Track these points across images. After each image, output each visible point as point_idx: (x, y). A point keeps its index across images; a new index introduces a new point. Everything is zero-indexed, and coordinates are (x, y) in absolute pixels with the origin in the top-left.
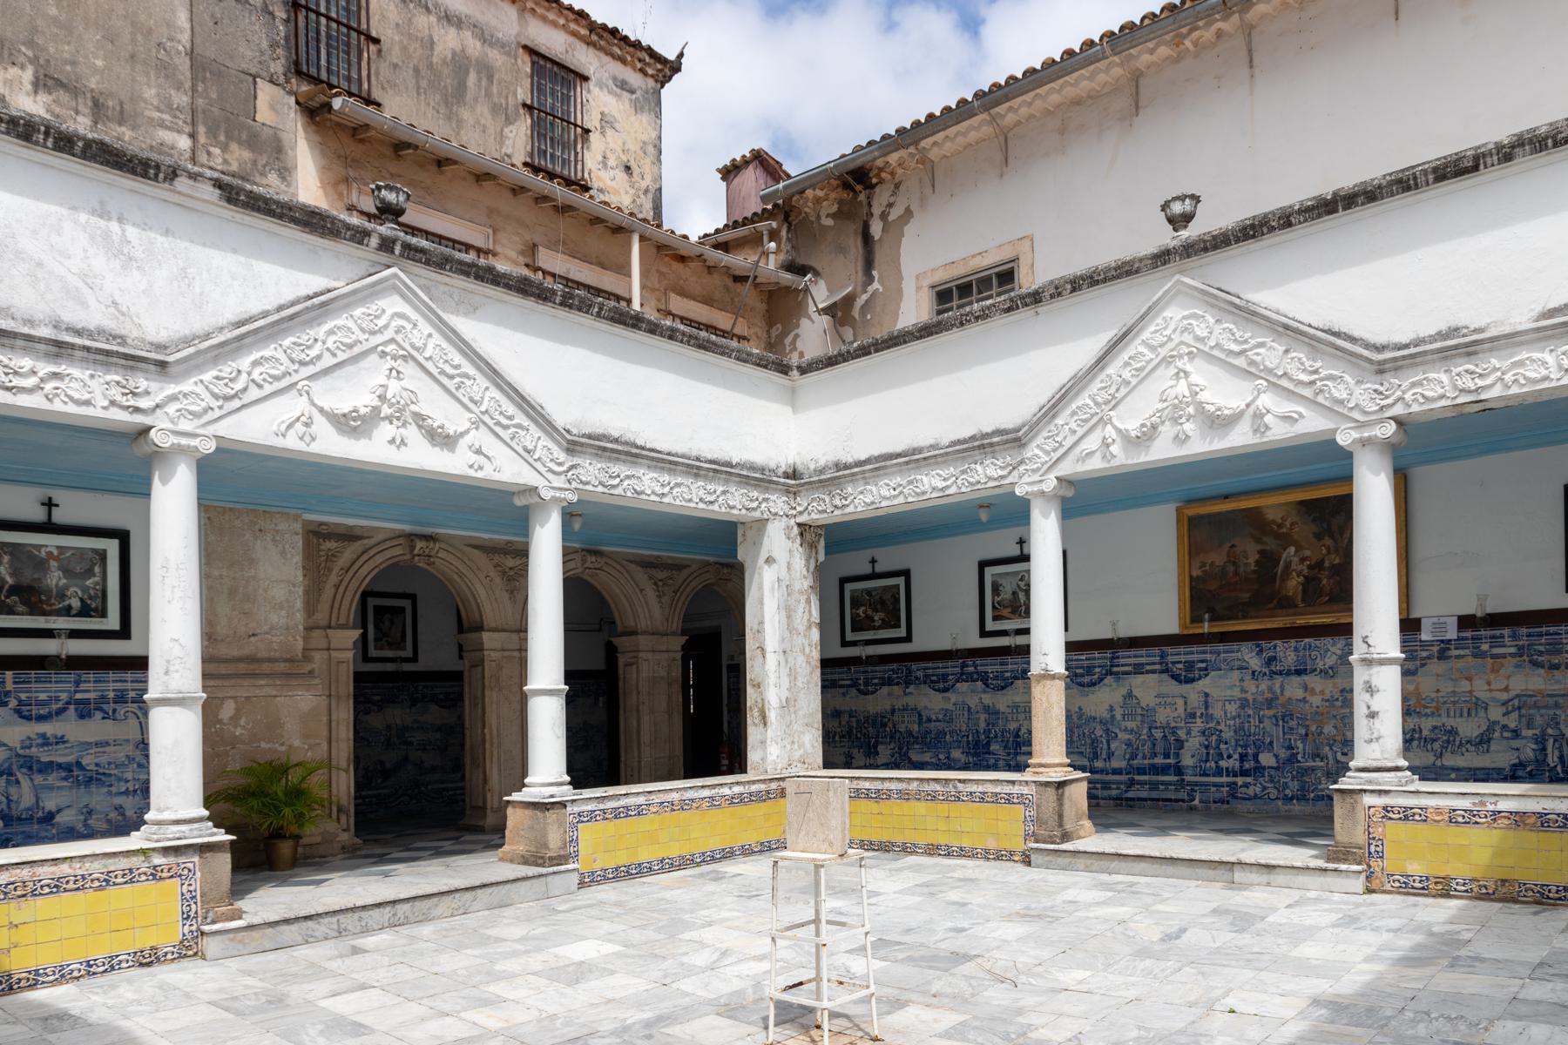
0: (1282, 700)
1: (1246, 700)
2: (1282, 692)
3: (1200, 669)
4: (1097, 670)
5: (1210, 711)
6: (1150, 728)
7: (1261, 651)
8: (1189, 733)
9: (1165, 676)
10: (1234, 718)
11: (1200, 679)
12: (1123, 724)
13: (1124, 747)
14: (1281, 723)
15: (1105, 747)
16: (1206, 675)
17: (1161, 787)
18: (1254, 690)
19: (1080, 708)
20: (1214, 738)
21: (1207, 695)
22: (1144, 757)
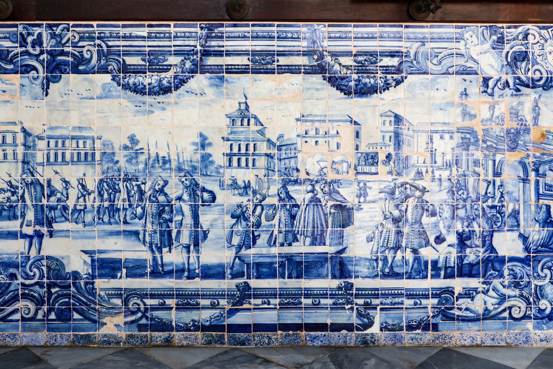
0: (534, 135)
1: (472, 132)
2: (536, 119)
3: (387, 70)
4: (173, 60)
5: (405, 151)
6: (285, 184)
7: (501, 40)
8: (362, 193)
9: (317, 79)
10: (448, 166)
11: (387, 86)
12: (228, 175)
13: (229, 221)
14: (532, 176)
15: (188, 220)
16: (398, 83)
17: (305, 301)
18: (485, 113)
19: (133, 139)
20: (411, 202)
21: (398, 119)
22: (271, 242)
